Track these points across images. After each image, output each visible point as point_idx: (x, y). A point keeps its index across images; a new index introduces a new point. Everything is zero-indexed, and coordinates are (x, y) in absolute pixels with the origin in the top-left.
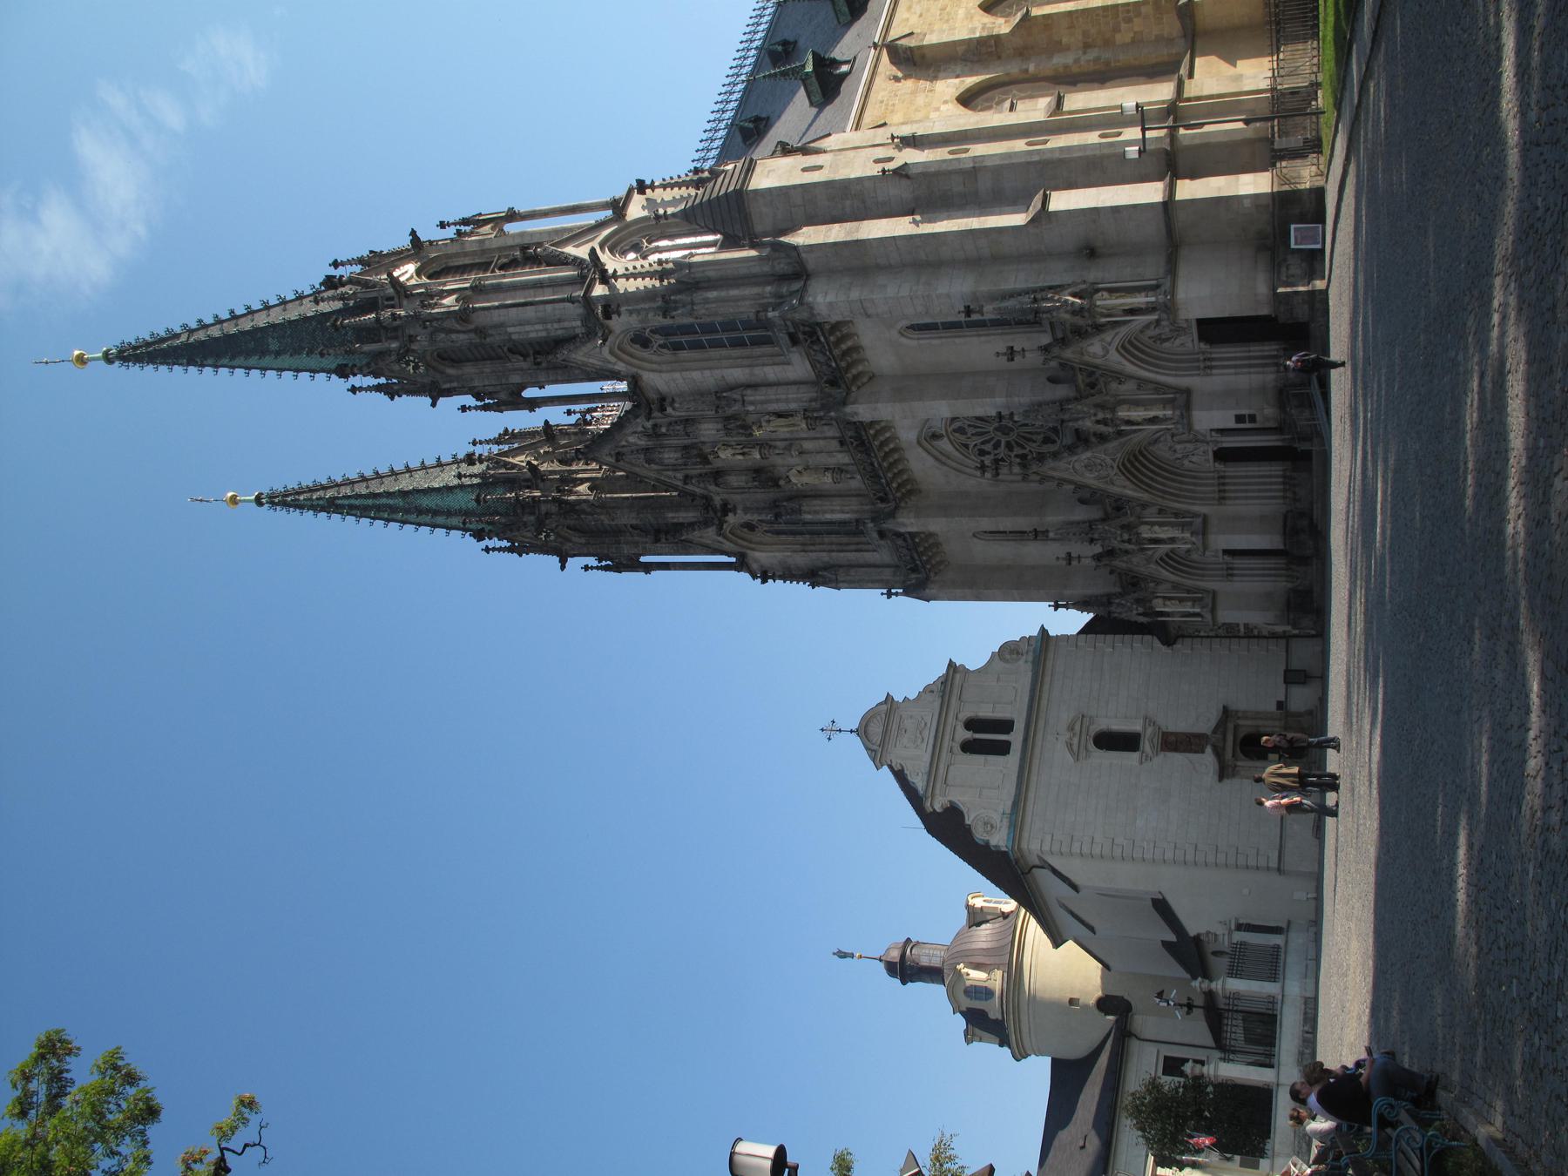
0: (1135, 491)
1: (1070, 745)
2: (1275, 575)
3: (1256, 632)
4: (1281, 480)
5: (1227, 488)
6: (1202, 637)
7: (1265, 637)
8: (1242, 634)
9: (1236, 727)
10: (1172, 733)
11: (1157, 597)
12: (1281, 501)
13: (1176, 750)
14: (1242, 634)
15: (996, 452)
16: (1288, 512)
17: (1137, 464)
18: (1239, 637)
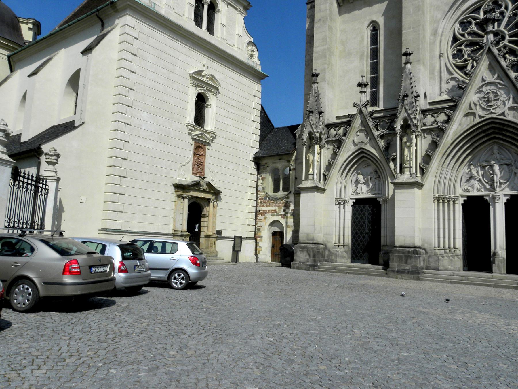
0: (455, 132)
1: (199, 73)
2: (339, 235)
3: (260, 217)
4: (452, 246)
5: (446, 204)
6: (257, 182)
7: (256, 224)
8: (259, 208)
9: (209, 200)
10: (205, 152)
11: (320, 148)
12: (437, 246)
13: (195, 154)
14: (259, 208)
15: (466, 35)
16: (424, 249)
17: (483, 135)
18: (256, 207)
